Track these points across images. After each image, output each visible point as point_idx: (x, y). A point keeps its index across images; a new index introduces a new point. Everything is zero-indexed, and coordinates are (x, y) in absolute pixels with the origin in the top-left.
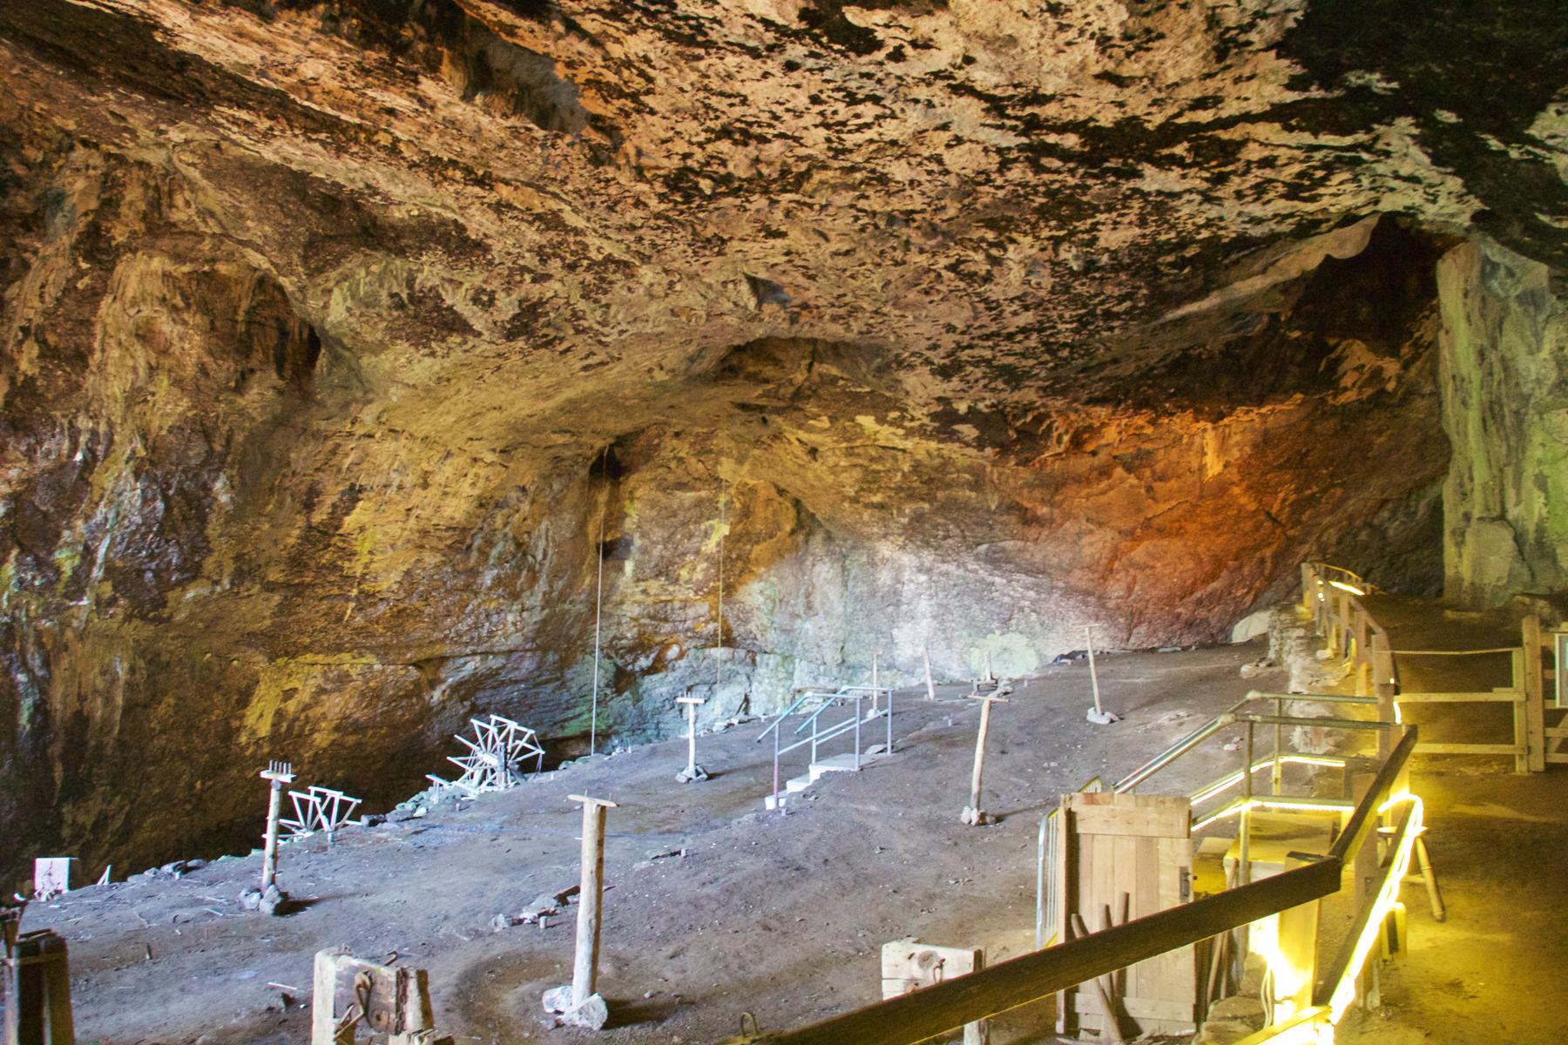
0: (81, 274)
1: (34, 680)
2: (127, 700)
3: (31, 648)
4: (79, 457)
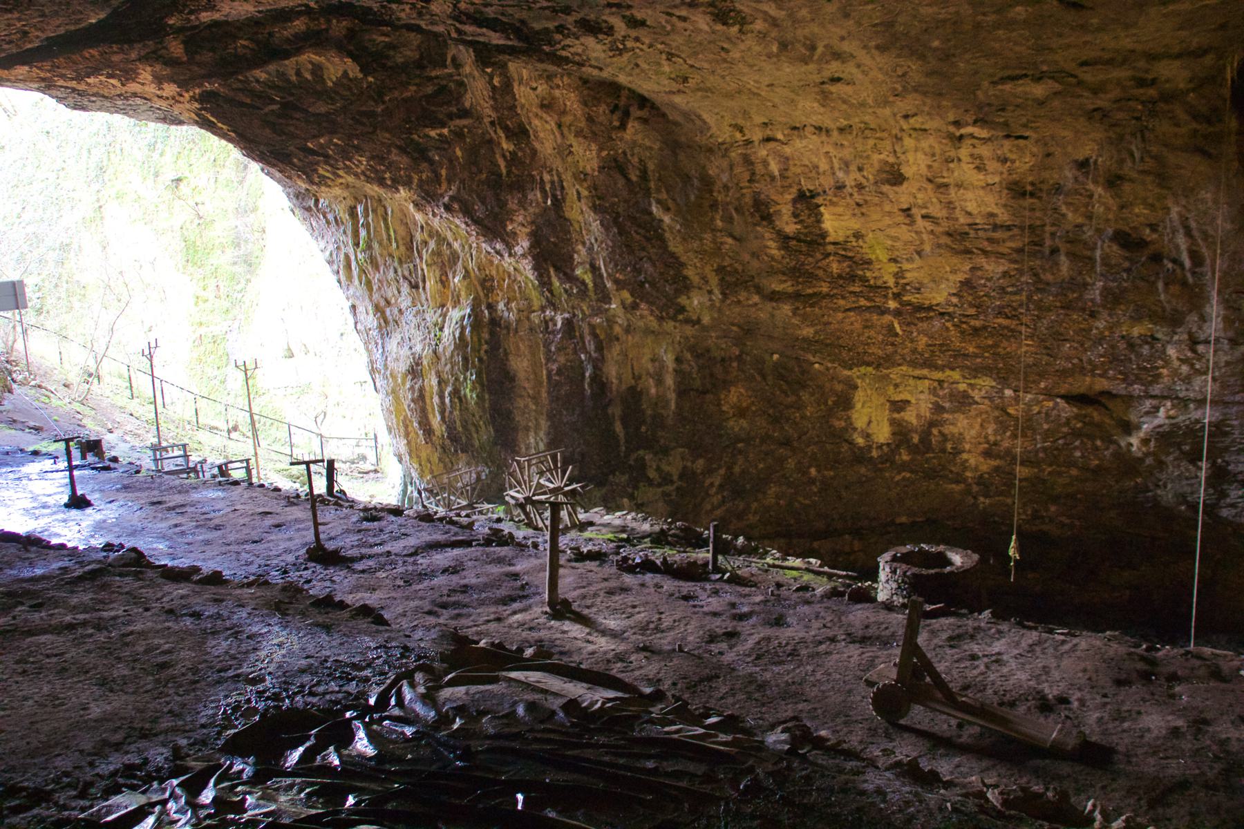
0: (491, 77)
1: (590, 358)
2: (678, 384)
3: (588, 338)
4: (549, 202)
